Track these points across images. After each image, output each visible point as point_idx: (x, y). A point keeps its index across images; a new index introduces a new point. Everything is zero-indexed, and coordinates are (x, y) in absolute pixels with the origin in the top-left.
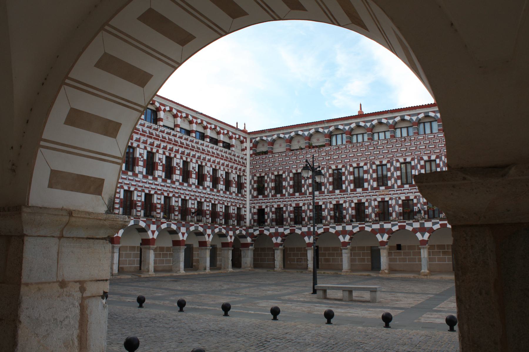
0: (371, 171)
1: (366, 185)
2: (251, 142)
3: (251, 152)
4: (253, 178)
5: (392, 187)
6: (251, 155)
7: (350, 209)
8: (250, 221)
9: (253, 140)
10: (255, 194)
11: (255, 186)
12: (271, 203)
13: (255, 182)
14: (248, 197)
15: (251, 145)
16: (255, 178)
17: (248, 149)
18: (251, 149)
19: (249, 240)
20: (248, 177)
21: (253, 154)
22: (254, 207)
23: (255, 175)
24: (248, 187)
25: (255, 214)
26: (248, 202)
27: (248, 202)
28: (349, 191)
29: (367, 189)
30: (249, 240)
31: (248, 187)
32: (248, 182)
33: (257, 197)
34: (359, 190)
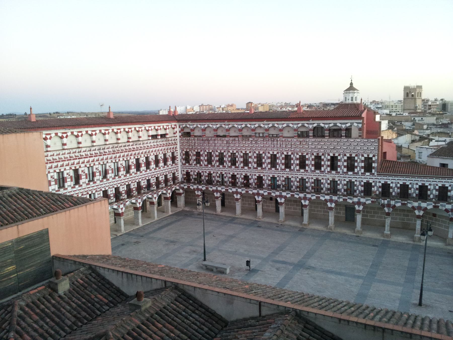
0: (253, 157)
1: (250, 165)
2: (180, 127)
3: (180, 134)
4: (182, 152)
5: (265, 168)
6: (180, 136)
7: (241, 179)
8: (182, 179)
9: (181, 126)
10: (184, 162)
11: (184, 157)
12: (194, 169)
13: (183, 155)
14: (180, 164)
15: (180, 130)
16: (184, 152)
17: (178, 132)
18: (180, 132)
20: (179, 151)
22: (184, 171)
23: (183, 150)
24: (179, 158)
25: (184, 175)
29: (250, 168)
31: (179, 158)
32: (179, 154)
33: (185, 164)
34: (246, 168)
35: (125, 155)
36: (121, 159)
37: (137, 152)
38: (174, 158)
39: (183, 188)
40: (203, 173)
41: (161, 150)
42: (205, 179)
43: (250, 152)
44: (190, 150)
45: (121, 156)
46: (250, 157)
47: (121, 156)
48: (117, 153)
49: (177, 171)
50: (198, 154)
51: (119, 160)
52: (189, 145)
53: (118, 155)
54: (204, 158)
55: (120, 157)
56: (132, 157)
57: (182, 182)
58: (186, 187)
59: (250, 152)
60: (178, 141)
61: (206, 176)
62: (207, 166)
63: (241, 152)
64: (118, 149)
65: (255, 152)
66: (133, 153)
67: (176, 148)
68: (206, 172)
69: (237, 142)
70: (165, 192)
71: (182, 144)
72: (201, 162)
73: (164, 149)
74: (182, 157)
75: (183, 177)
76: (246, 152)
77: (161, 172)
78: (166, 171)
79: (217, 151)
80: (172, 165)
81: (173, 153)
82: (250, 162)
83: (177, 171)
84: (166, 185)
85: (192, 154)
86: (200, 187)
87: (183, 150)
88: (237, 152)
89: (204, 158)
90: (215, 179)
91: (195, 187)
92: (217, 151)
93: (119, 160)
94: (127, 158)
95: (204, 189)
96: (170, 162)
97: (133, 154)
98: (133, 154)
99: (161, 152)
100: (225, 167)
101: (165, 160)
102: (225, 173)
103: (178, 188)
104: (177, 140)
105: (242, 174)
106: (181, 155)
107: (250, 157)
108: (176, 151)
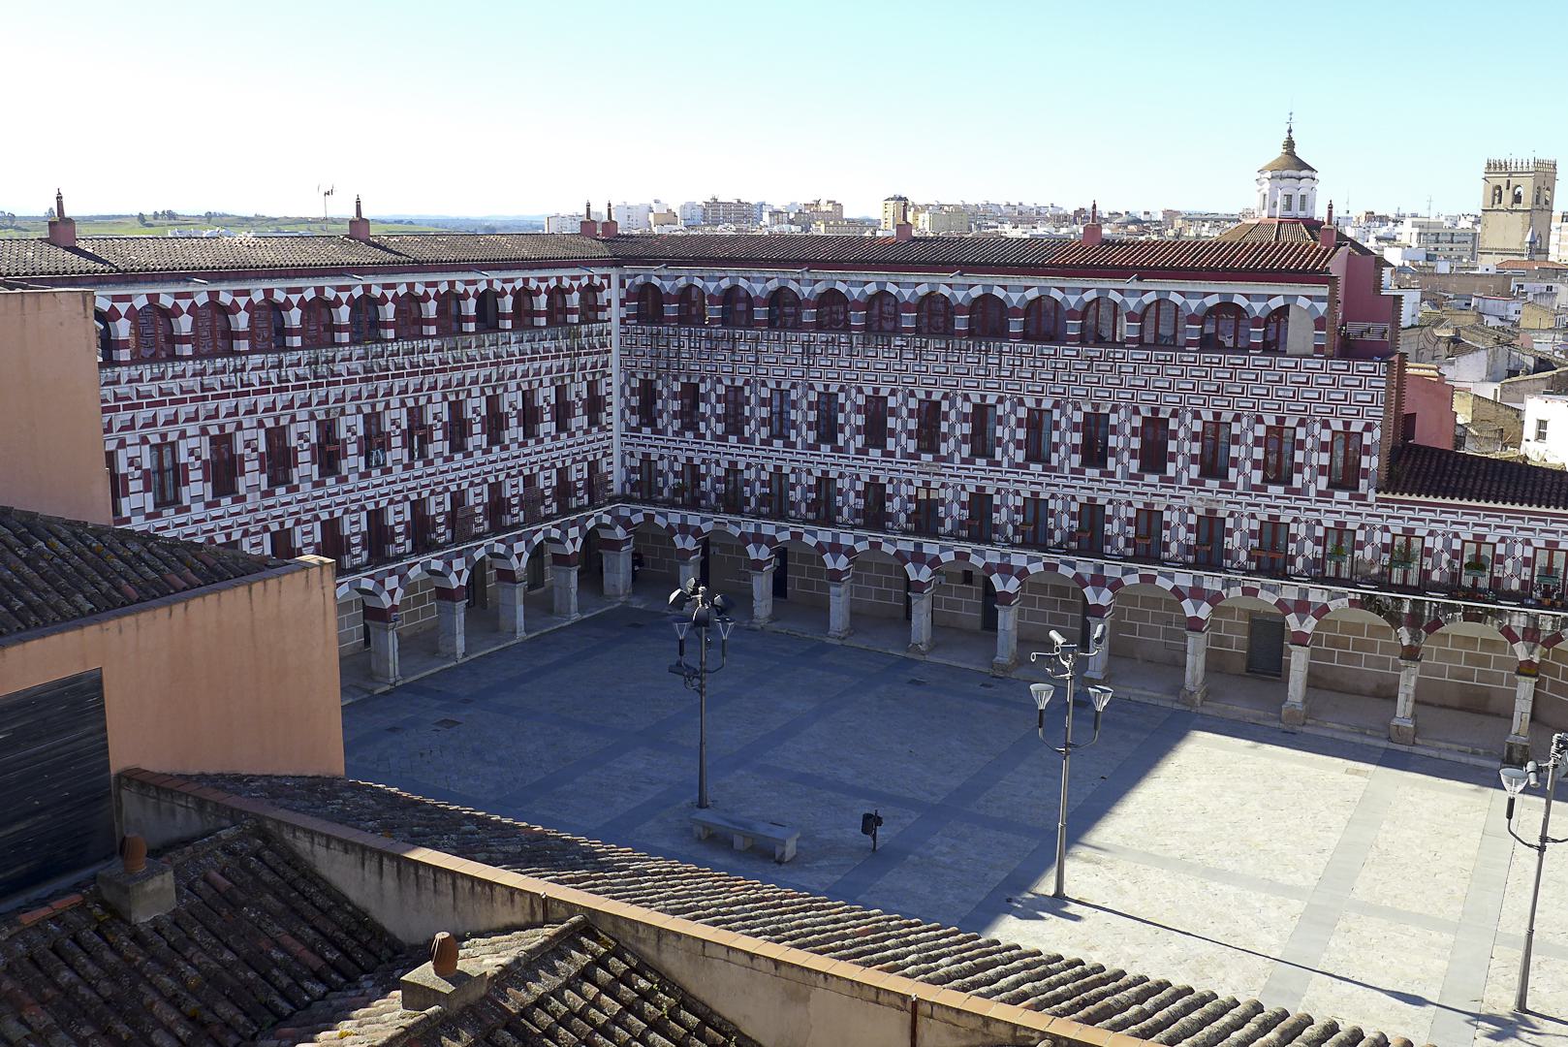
0: (905, 412)
1: (891, 443)
2: (622, 284)
3: (624, 313)
6: (623, 321)
8: (623, 485)
9: (628, 282)
10: (634, 421)
11: (635, 401)
14: (617, 427)
15: (623, 296)
17: (615, 303)
18: (622, 303)
19: (620, 533)
20: (616, 378)
21: (629, 317)
22: (632, 455)
26: (616, 441)
27: (616, 441)
28: (852, 451)
30: (620, 533)
32: (615, 389)
35: (411, 388)
36: (395, 402)
37: (457, 375)
38: (595, 405)
39: (626, 523)
40: (708, 468)
41: (549, 372)
42: (714, 489)
43: (893, 393)
44: (659, 377)
45: (396, 390)
46: (893, 412)
47: (396, 390)
48: (379, 378)
49: (605, 455)
50: (691, 395)
51: (387, 406)
52: (659, 356)
53: (383, 385)
54: (713, 408)
55: (389, 393)
56: (437, 396)
57: (626, 499)
58: (638, 519)
59: (893, 393)
60: (615, 338)
61: (718, 479)
62: (723, 438)
63: (860, 390)
64: (382, 361)
65: (912, 394)
66: (441, 378)
67: (605, 365)
68: (718, 464)
69: (844, 350)
70: (556, 534)
71: (628, 351)
72: (702, 425)
73: (561, 370)
74: (628, 401)
75: (628, 480)
76: (876, 390)
77: (544, 456)
78: (565, 452)
79: (764, 384)
80: (587, 432)
81: (592, 386)
82: (892, 433)
83: (605, 455)
84: (564, 510)
85: (668, 389)
86: (694, 519)
87: (633, 375)
88: (842, 389)
89: (713, 408)
90: (752, 493)
91: (675, 518)
92: (764, 384)
93: (387, 406)
94: (416, 400)
95: (707, 527)
96: (579, 420)
97: (440, 385)
98: (440, 385)
99: (546, 381)
100: (793, 445)
101: (562, 412)
102: (793, 471)
103: (607, 519)
104: (609, 333)
105: (858, 478)
106: (622, 395)
107: (893, 412)
108: (604, 375)
